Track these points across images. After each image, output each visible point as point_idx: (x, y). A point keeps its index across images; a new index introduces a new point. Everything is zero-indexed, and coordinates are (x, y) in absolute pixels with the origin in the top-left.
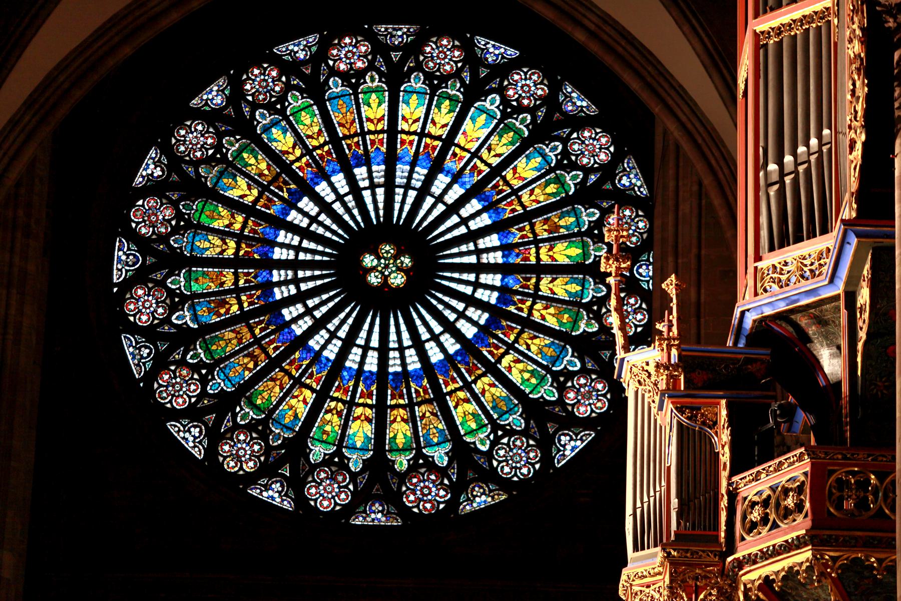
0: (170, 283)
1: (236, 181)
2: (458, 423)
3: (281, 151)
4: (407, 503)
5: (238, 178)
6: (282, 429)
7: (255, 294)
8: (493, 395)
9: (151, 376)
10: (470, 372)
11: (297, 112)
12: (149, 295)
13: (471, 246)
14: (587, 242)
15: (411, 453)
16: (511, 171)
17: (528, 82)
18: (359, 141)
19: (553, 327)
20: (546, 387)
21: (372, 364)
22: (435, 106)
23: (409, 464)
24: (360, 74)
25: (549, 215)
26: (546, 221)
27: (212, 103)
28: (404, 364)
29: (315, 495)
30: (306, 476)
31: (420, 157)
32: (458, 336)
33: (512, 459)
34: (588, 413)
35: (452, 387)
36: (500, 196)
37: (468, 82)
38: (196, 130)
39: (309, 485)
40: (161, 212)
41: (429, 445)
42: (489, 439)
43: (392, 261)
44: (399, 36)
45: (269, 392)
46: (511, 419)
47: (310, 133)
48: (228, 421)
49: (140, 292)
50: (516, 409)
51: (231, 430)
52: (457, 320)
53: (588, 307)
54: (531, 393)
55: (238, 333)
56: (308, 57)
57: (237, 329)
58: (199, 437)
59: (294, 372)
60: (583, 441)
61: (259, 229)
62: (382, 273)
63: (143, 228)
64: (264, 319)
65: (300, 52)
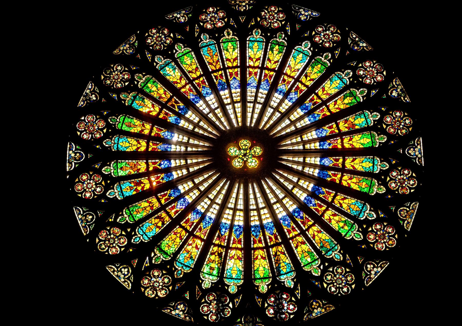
2: (299, 258)
4: (269, 315)
5: (146, 100)
6: (182, 267)
7: (160, 176)
9: (94, 234)
10: (304, 223)
11: (181, 56)
12: (90, 180)
13: (299, 139)
15: (269, 280)
16: (321, 90)
18: (222, 73)
21: (239, 221)
22: (270, 50)
23: (268, 288)
24: (221, 31)
26: (346, 121)
27: (126, 52)
28: (260, 220)
29: (207, 312)
30: (201, 299)
31: (262, 83)
33: (336, 282)
35: (293, 234)
37: (289, 34)
38: (117, 70)
39: (203, 305)
40: (96, 124)
42: (320, 268)
43: (248, 151)
44: (244, 6)
45: (173, 242)
46: (333, 254)
47: (191, 70)
48: (147, 263)
50: (336, 247)
55: (150, 203)
58: (127, 275)
59: (188, 228)
60: (382, 268)
61: (161, 133)
62: (243, 159)
63: (85, 135)
64: (167, 193)
65: (181, 18)
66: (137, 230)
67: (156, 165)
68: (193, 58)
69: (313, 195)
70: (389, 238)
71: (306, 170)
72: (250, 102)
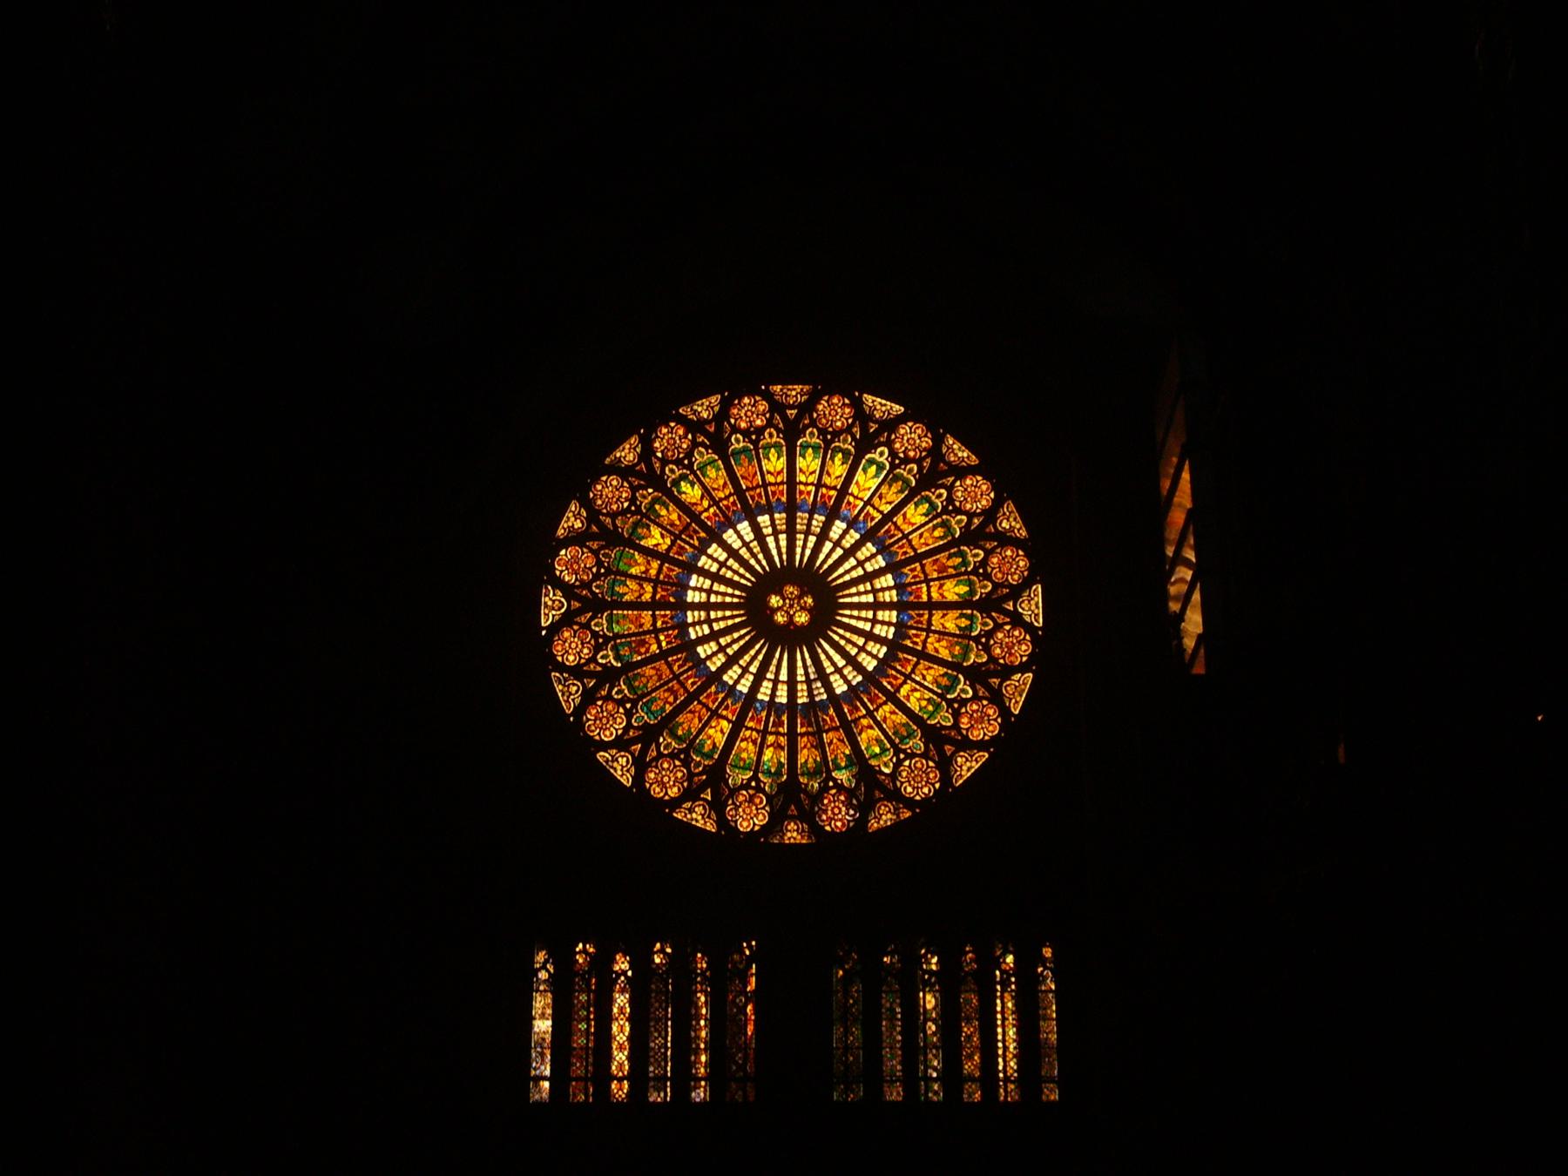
0: (595, 625)
1: (650, 531)
2: (863, 748)
3: (690, 503)
5: (652, 528)
8: (893, 722)
12: (574, 637)
14: (974, 581)
16: (902, 517)
17: (913, 435)
18: (760, 493)
19: (945, 658)
20: (942, 714)
24: (760, 431)
25: (938, 557)
26: (935, 562)
32: (859, 668)
33: (914, 779)
34: (981, 736)
36: (892, 540)
41: (838, 768)
44: (793, 396)
46: (911, 743)
47: (716, 486)
49: (566, 634)
50: (916, 734)
51: (656, 759)
52: (857, 654)
53: (977, 639)
54: (928, 718)
55: (658, 670)
56: (711, 417)
57: (658, 667)
59: (711, 705)
60: (977, 762)
63: (566, 576)
66: (639, 707)
67: (666, 619)
68: (720, 469)
69: (884, 663)
70: (989, 723)
71: (878, 630)
72: (800, 533)
